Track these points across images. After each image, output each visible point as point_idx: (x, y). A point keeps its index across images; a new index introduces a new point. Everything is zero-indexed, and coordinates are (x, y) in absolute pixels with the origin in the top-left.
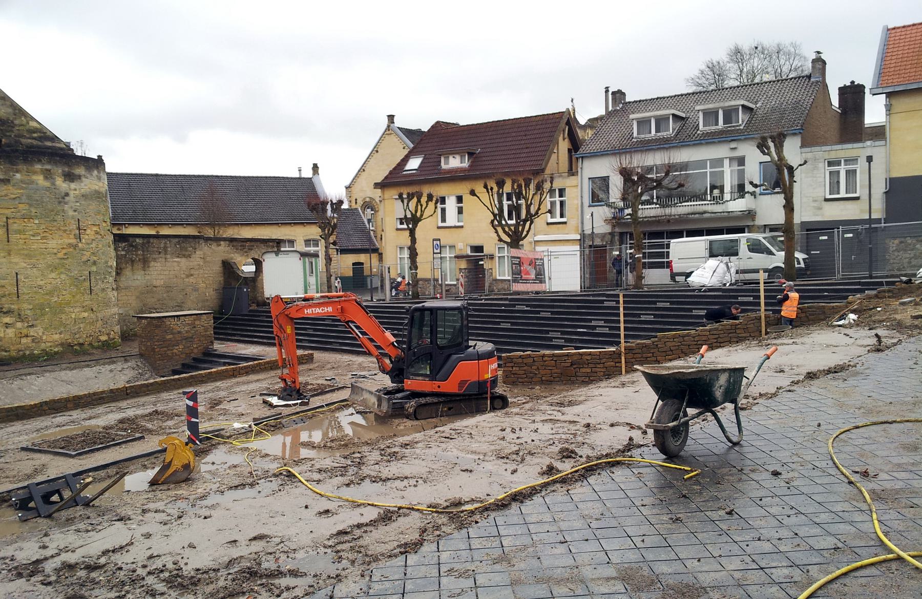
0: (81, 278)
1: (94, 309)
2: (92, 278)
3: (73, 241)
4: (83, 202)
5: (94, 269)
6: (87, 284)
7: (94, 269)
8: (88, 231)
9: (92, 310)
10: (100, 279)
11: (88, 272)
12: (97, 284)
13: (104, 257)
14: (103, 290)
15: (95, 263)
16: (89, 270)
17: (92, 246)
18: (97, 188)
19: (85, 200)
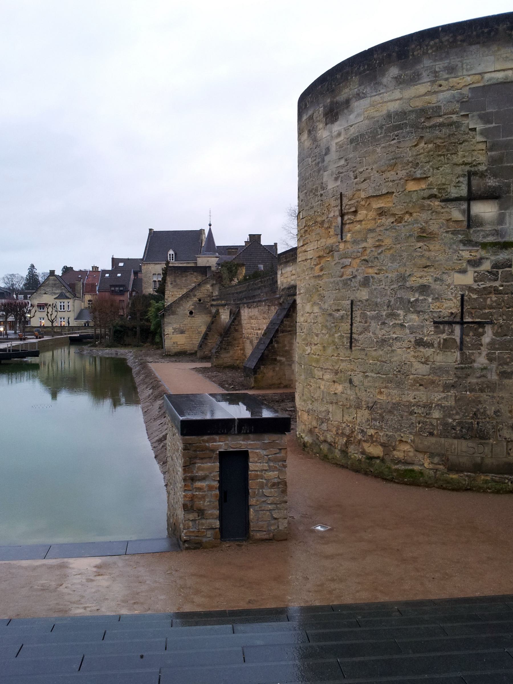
0: (337, 315)
1: (356, 381)
2: (357, 314)
3: (332, 241)
4: (351, 156)
5: (363, 294)
6: (345, 326)
7: (363, 294)
8: (362, 214)
9: (351, 382)
10: (377, 318)
11: (349, 302)
12: (366, 329)
13: (395, 265)
14: (384, 341)
15: (366, 282)
16: (351, 298)
17: (364, 245)
18: (394, 107)
19: (355, 149)
